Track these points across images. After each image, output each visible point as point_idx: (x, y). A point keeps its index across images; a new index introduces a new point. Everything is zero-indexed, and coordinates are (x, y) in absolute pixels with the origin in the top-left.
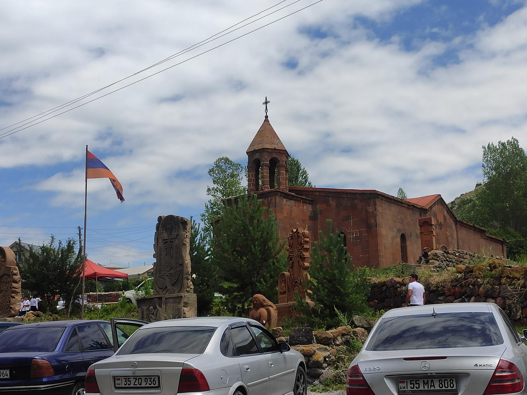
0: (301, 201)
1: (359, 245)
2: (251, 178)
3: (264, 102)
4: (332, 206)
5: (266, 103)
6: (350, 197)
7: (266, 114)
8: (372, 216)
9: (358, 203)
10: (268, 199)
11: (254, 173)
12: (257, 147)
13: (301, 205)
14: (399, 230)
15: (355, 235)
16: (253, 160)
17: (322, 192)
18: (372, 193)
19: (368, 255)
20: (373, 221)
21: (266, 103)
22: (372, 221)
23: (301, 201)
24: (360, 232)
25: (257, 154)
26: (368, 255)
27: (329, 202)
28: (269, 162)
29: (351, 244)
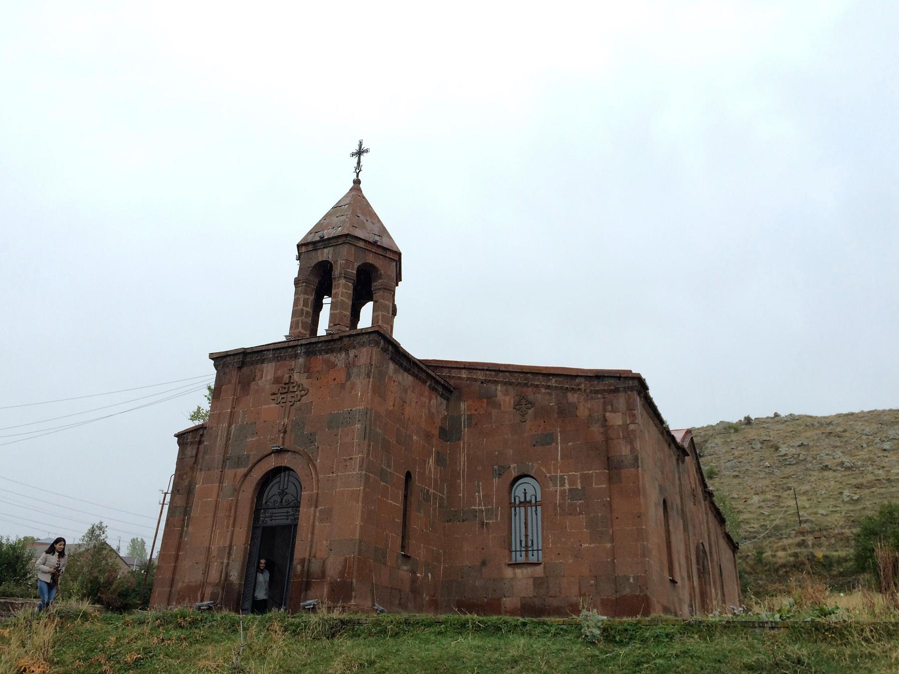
0: (428, 384)
1: (579, 514)
2: (300, 307)
3: (355, 151)
4: (502, 408)
5: (360, 153)
6: (557, 385)
7: (357, 176)
8: (621, 437)
9: (579, 402)
10: (347, 354)
11: (313, 297)
12: (328, 233)
13: (427, 393)
14: (662, 489)
15: (567, 487)
16: (313, 265)
17: (479, 372)
18: (625, 377)
19: (609, 545)
20: (625, 450)
21: (360, 153)
22: (623, 449)
23: (426, 382)
24: (586, 479)
25: (326, 250)
26: (609, 545)
27: (496, 396)
28: (355, 272)
29: (555, 509)
